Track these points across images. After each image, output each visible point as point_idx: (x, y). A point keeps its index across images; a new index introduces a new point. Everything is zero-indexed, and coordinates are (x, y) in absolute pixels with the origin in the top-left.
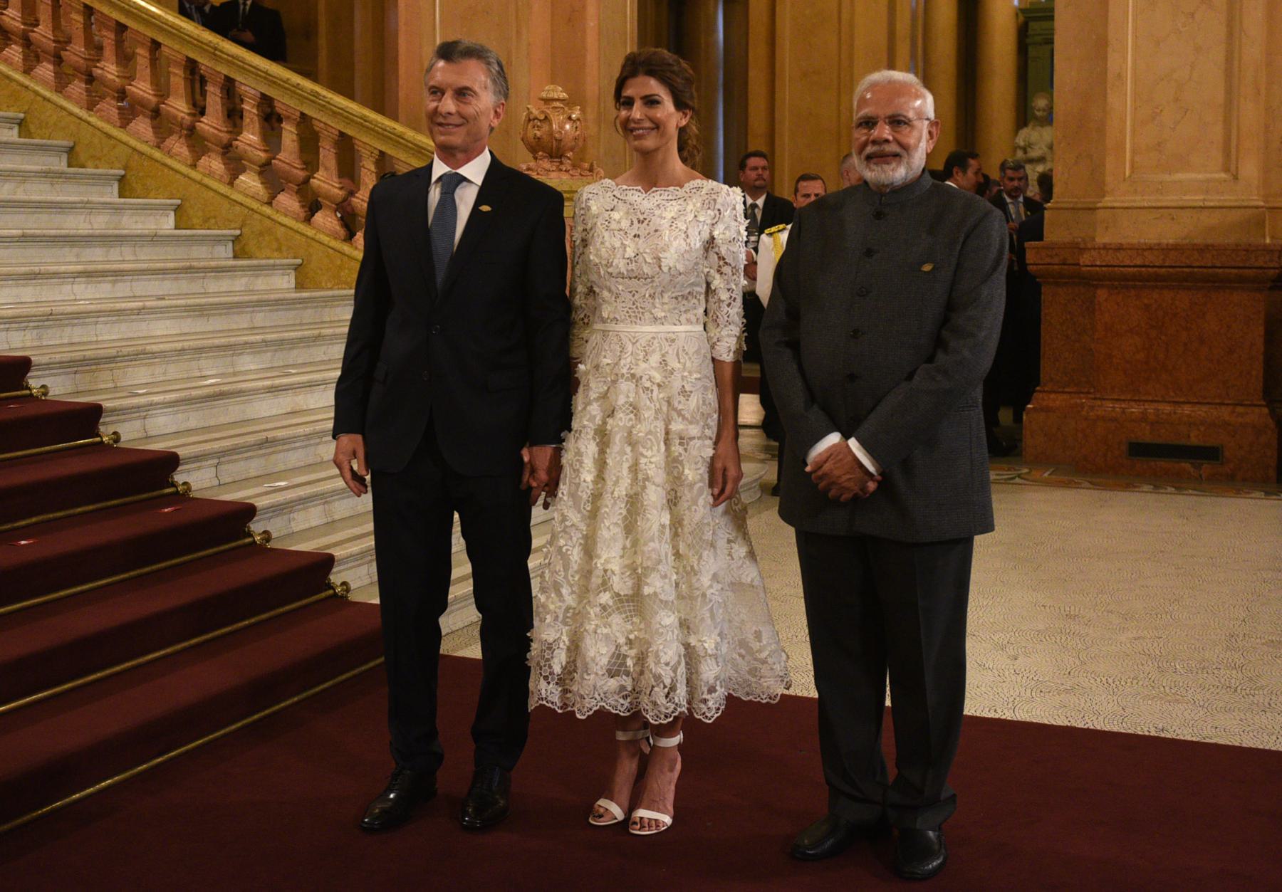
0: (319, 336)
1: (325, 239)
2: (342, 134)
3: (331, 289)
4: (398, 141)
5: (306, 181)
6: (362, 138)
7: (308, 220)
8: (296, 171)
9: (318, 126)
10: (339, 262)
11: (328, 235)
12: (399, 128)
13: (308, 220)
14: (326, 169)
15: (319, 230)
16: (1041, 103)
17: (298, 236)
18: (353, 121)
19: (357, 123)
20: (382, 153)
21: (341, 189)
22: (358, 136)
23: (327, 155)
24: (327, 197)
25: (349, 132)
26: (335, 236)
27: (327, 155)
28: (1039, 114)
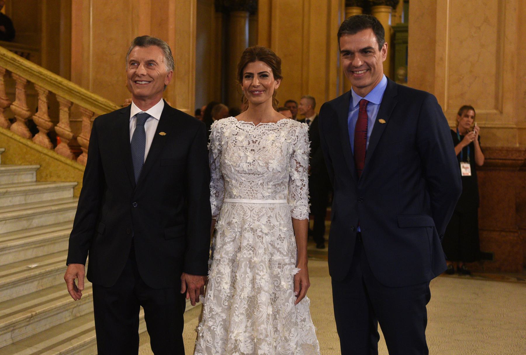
0: (7, 192)
1: (18, 138)
2: (28, 82)
3: (20, 165)
4: (58, 85)
5: (9, 106)
6: (39, 84)
7: (9, 128)
8: (2, 101)
9: (15, 77)
10: (25, 150)
11: (19, 136)
12: (59, 79)
13: (9, 128)
14: (19, 100)
15: (15, 133)
16: (401, 72)
17: (3, 136)
18: (34, 74)
19: (36, 75)
20: (50, 93)
21: (27, 111)
22: (37, 83)
23: (20, 92)
24: (20, 115)
25: (33, 80)
26: (23, 136)
27: (20, 92)
28: (400, 77)
